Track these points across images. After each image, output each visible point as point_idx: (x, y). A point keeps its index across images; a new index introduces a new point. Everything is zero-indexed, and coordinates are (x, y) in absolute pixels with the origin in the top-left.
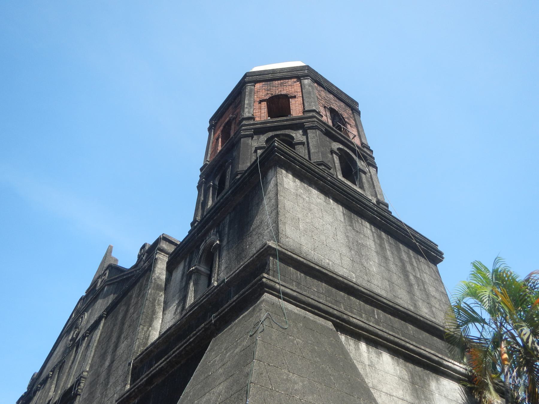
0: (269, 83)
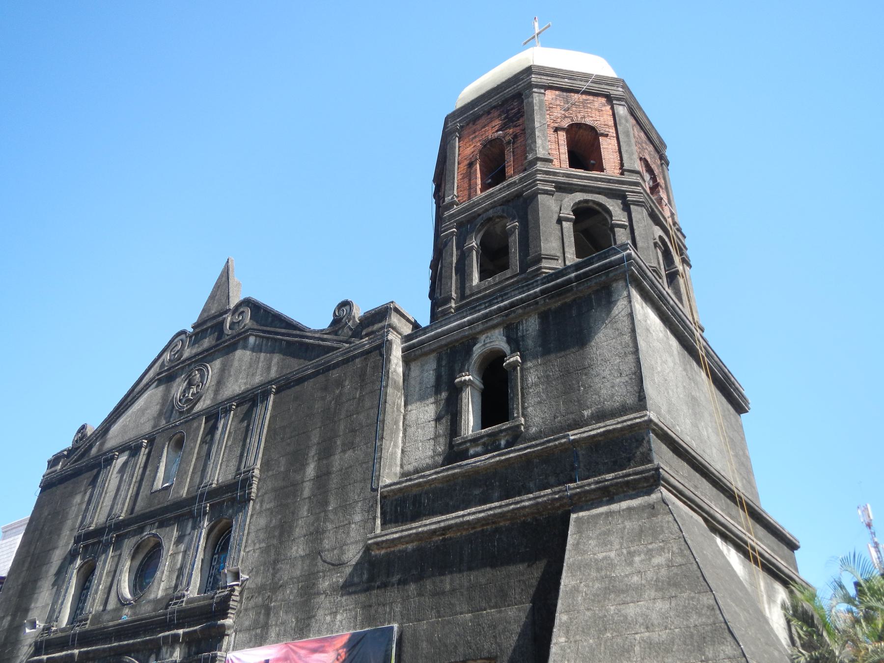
0: (565, 94)
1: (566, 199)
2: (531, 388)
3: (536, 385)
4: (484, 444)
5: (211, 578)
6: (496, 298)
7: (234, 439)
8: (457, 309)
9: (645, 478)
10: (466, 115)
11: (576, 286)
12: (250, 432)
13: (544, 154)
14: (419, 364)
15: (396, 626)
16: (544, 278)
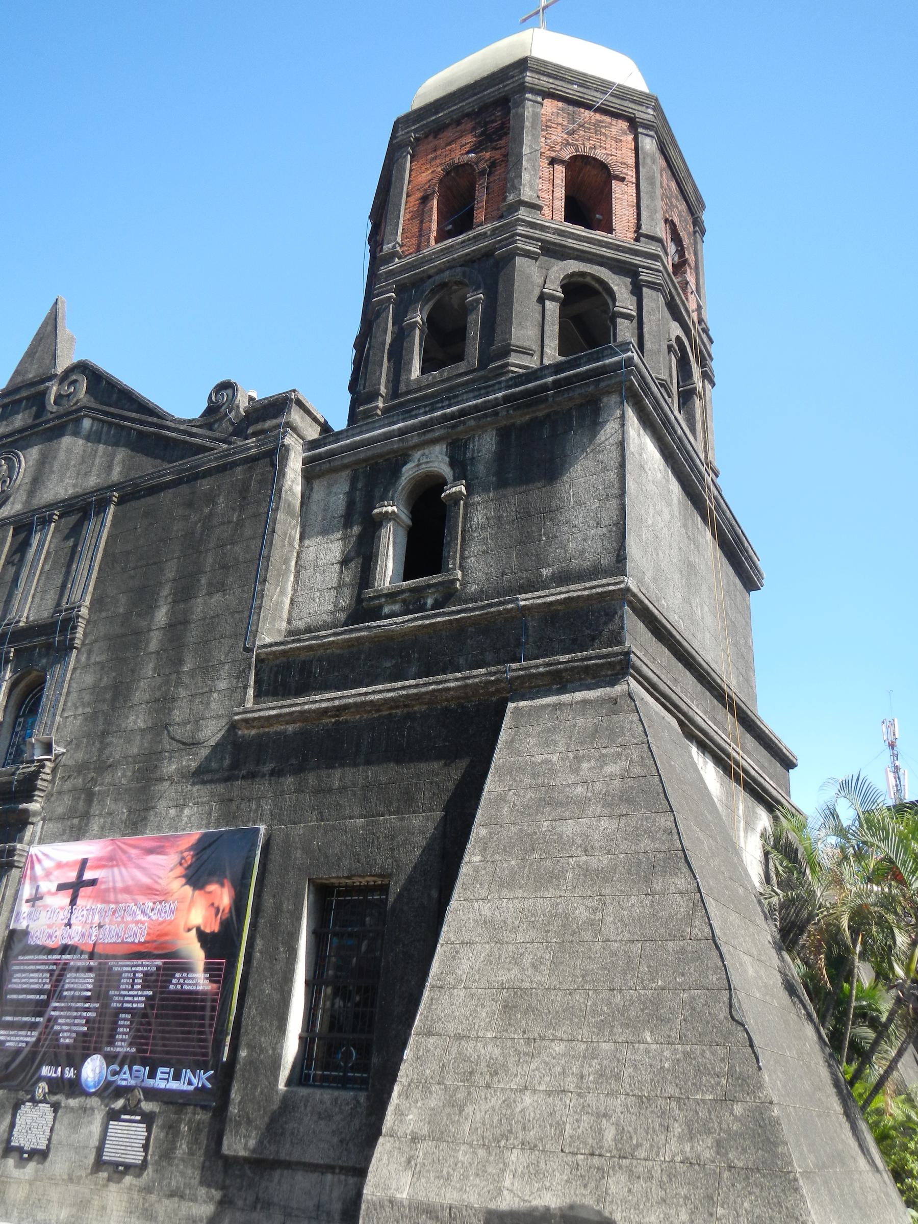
0: (571, 108)
1: (555, 268)
2: (475, 531)
3: (483, 528)
4: (404, 601)
5: (13, 747)
6: (441, 400)
7: (54, 562)
8: (386, 411)
9: (609, 663)
10: (425, 122)
11: (553, 395)
12: (77, 555)
13: (531, 197)
15: (263, 828)
16: (511, 378)
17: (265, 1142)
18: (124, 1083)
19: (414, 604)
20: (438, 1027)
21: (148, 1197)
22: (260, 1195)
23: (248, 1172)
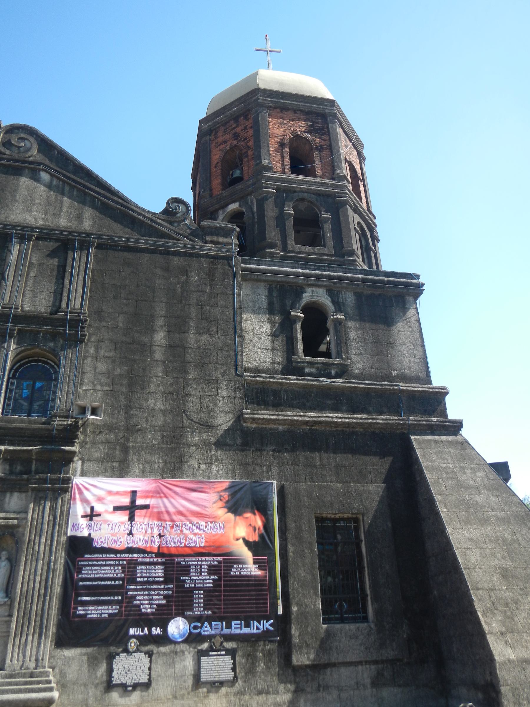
6: (324, 266)
11: (387, 287)
14: (250, 285)
15: (275, 483)
17: (321, 655)
18: (207, 633)
19: (323, 371)
20: (480, 585)
21: (242, 697)
22: (321, 683)
23: (310, 672)
